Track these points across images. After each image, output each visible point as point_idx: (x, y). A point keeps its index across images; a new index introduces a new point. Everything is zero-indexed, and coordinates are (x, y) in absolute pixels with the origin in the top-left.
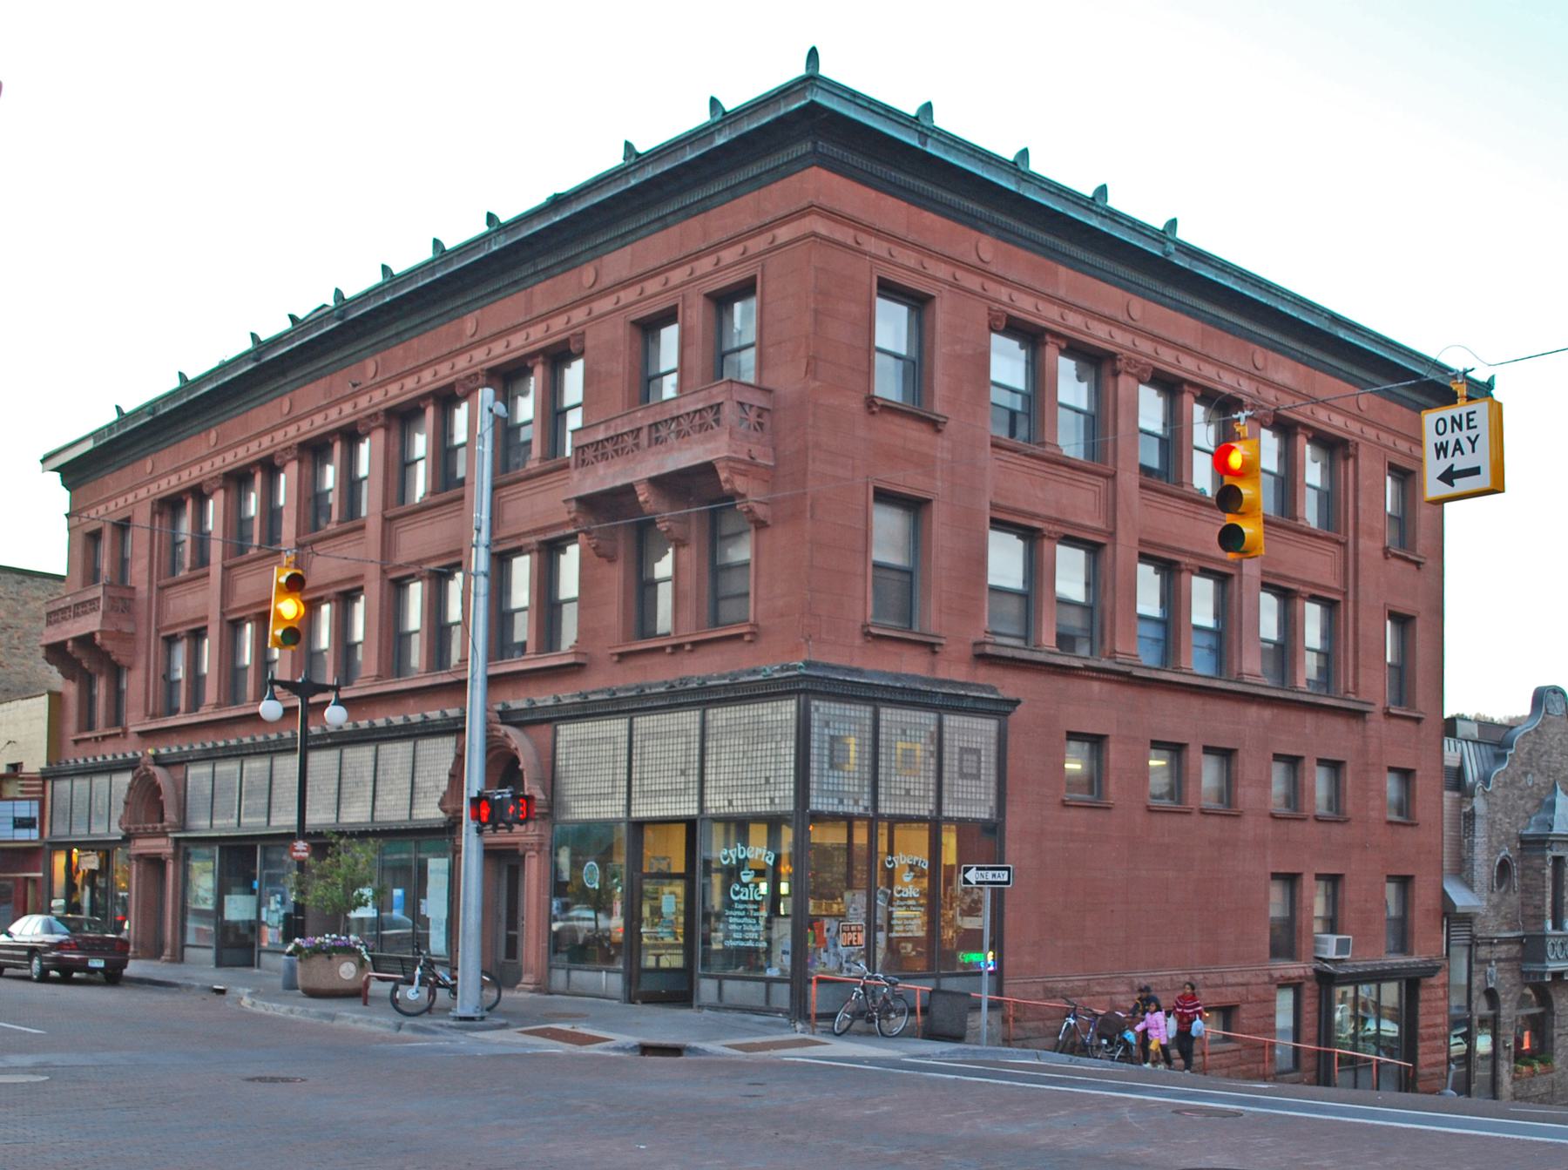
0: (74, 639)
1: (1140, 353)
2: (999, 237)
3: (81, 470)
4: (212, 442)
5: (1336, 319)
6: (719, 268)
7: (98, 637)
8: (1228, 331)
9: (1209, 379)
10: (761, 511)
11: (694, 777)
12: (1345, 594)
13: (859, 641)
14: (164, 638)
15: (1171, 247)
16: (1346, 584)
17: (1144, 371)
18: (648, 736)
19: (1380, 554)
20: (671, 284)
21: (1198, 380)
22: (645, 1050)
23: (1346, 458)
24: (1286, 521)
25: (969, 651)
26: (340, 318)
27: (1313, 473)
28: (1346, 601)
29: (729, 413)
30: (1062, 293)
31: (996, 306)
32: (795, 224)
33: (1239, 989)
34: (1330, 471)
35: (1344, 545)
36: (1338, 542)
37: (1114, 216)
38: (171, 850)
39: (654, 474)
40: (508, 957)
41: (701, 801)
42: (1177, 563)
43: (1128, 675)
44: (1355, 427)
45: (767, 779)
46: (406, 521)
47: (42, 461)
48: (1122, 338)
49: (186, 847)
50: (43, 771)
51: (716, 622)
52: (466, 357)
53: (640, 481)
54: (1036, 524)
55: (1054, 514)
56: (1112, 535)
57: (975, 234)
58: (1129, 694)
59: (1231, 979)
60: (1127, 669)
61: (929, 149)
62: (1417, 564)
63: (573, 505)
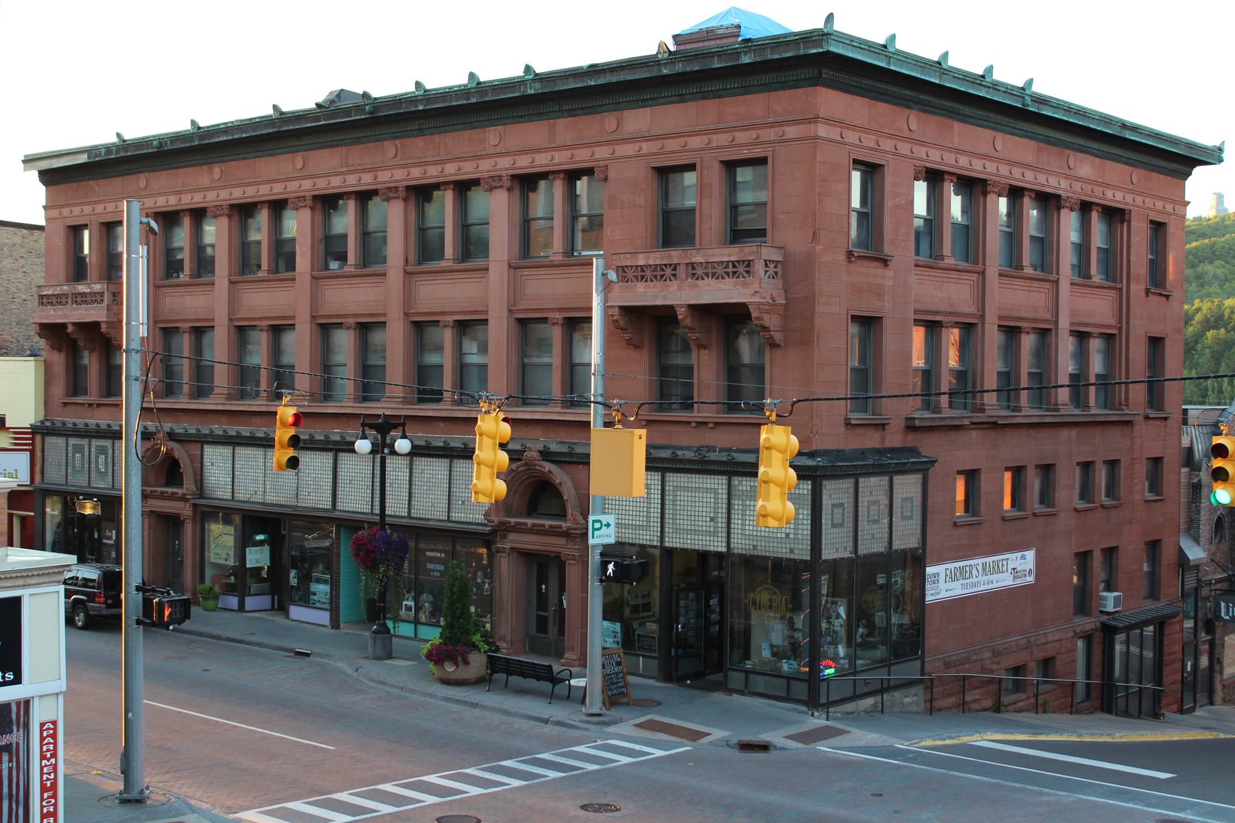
0: (74, 324)
1: (1002, 176)
2: (921, 110)
3: (61, 175)
4: (217, 177)
5: (1124, 125)
6: (733, 143)
7: (103, 326)
8: (1053, 144)
9: (1043, 185)
10: (778, 337)
11: (722, 523)
12: (1120, 329)
13: (843, 430)
14: (163, 329)
15: (1028, 100)
16: (1121, 322)
17: (1003, 188)
18: (676, 488)
19: (1143, 293)
20: (688, 147)
21: (1035, 187)
22: (746, 747)
23: (1122, 222)
24: (1086, 281)
25: (902, 423)
26: (371, 113)
27: (1098, 238)
28: (1120, 333)
29: (759, 267)
30: (956, 146)
31: (918, 163)
32: (801, 127)
33: (1057, 644)
34: (1111, 235)
35: (1121, 289)
36: (1115, 289)
37: (996, 86)
38: (190, 513)
39: (692, 302)
40: (538, 631)
41: (728, 542)
42: (1019, 328)
43: (995, 423)
44: (1129, 198)
45: (787, 535)
46: (422, 277)
47: (24, 162)
48: (991, 167)
49: (208, 512)
50: (33, 427)
51: (733, 408)
52: (492, 161)
53: (681, 306)
54: (938, 318)
55: (949, 310)
56: (983, 316)
57: (907, 111)
58: (992, 435)
59: (1051, 638)
60: (994, 420)
61: (892, 68)
62: (1167, 297)
63: (616, 311)
